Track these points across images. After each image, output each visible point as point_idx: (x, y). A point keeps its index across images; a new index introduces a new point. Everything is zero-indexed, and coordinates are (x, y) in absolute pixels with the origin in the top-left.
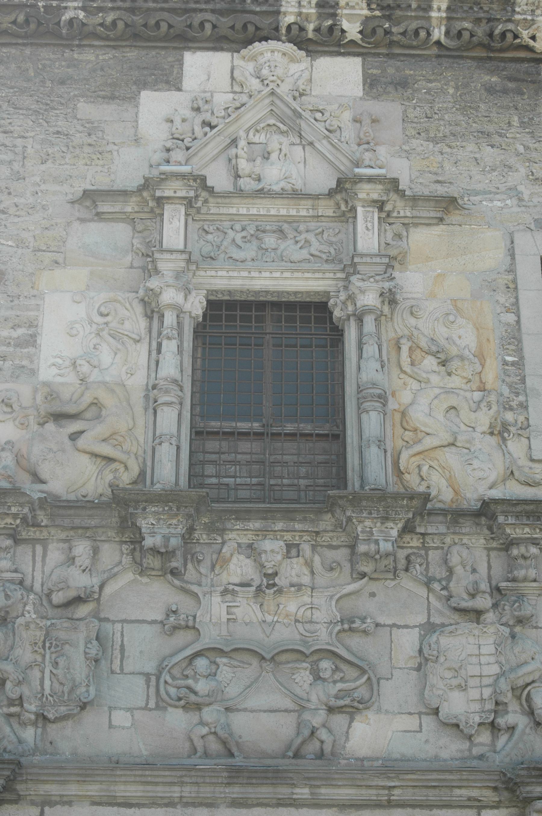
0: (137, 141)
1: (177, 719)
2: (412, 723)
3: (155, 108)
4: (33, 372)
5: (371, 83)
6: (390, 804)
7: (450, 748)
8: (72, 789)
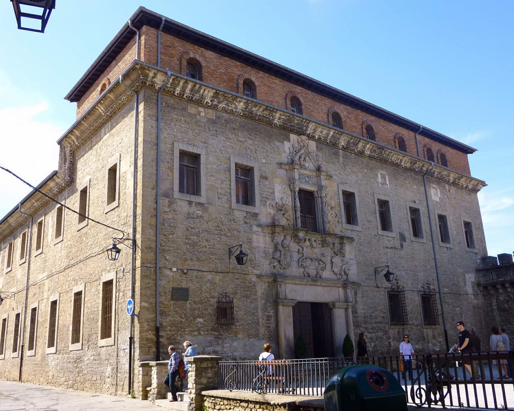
0: (285, 152)
1: (302, 270)
2: (330, 273)
3: (287, 145)
4: (275, 200)
5: (317, 148)
6: (329, 286)
7: (335, 277)
8: (290, 281)
